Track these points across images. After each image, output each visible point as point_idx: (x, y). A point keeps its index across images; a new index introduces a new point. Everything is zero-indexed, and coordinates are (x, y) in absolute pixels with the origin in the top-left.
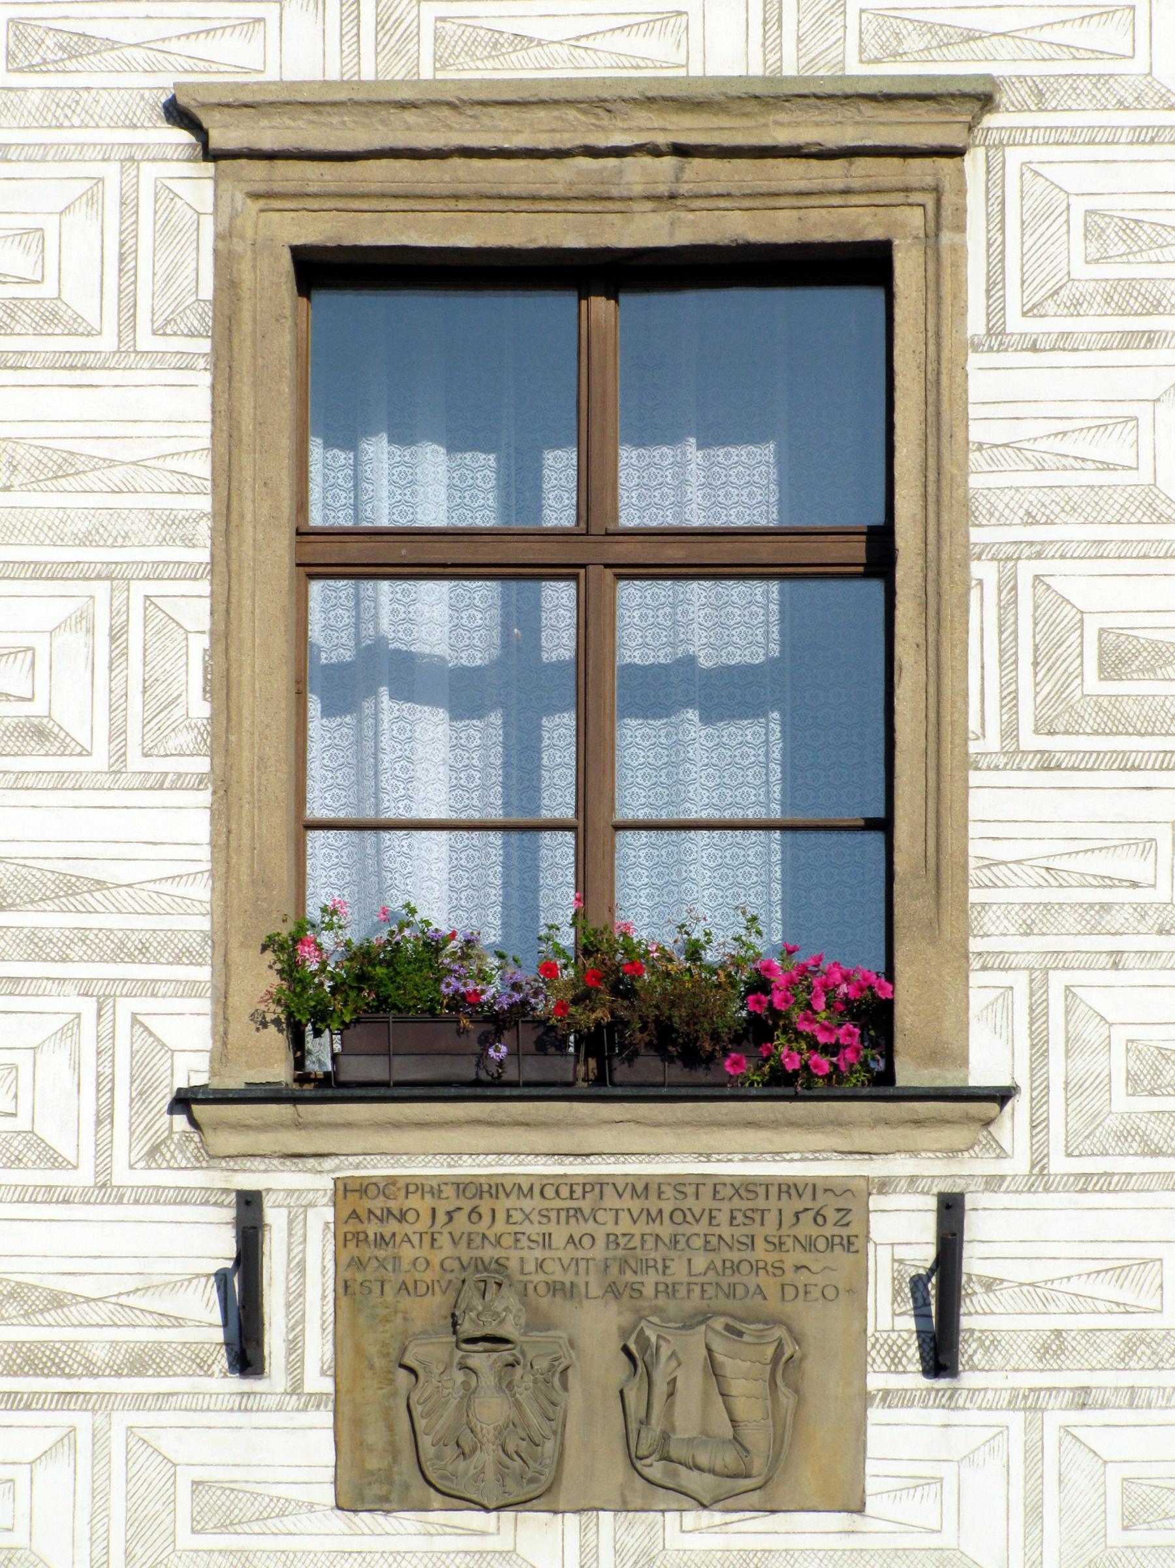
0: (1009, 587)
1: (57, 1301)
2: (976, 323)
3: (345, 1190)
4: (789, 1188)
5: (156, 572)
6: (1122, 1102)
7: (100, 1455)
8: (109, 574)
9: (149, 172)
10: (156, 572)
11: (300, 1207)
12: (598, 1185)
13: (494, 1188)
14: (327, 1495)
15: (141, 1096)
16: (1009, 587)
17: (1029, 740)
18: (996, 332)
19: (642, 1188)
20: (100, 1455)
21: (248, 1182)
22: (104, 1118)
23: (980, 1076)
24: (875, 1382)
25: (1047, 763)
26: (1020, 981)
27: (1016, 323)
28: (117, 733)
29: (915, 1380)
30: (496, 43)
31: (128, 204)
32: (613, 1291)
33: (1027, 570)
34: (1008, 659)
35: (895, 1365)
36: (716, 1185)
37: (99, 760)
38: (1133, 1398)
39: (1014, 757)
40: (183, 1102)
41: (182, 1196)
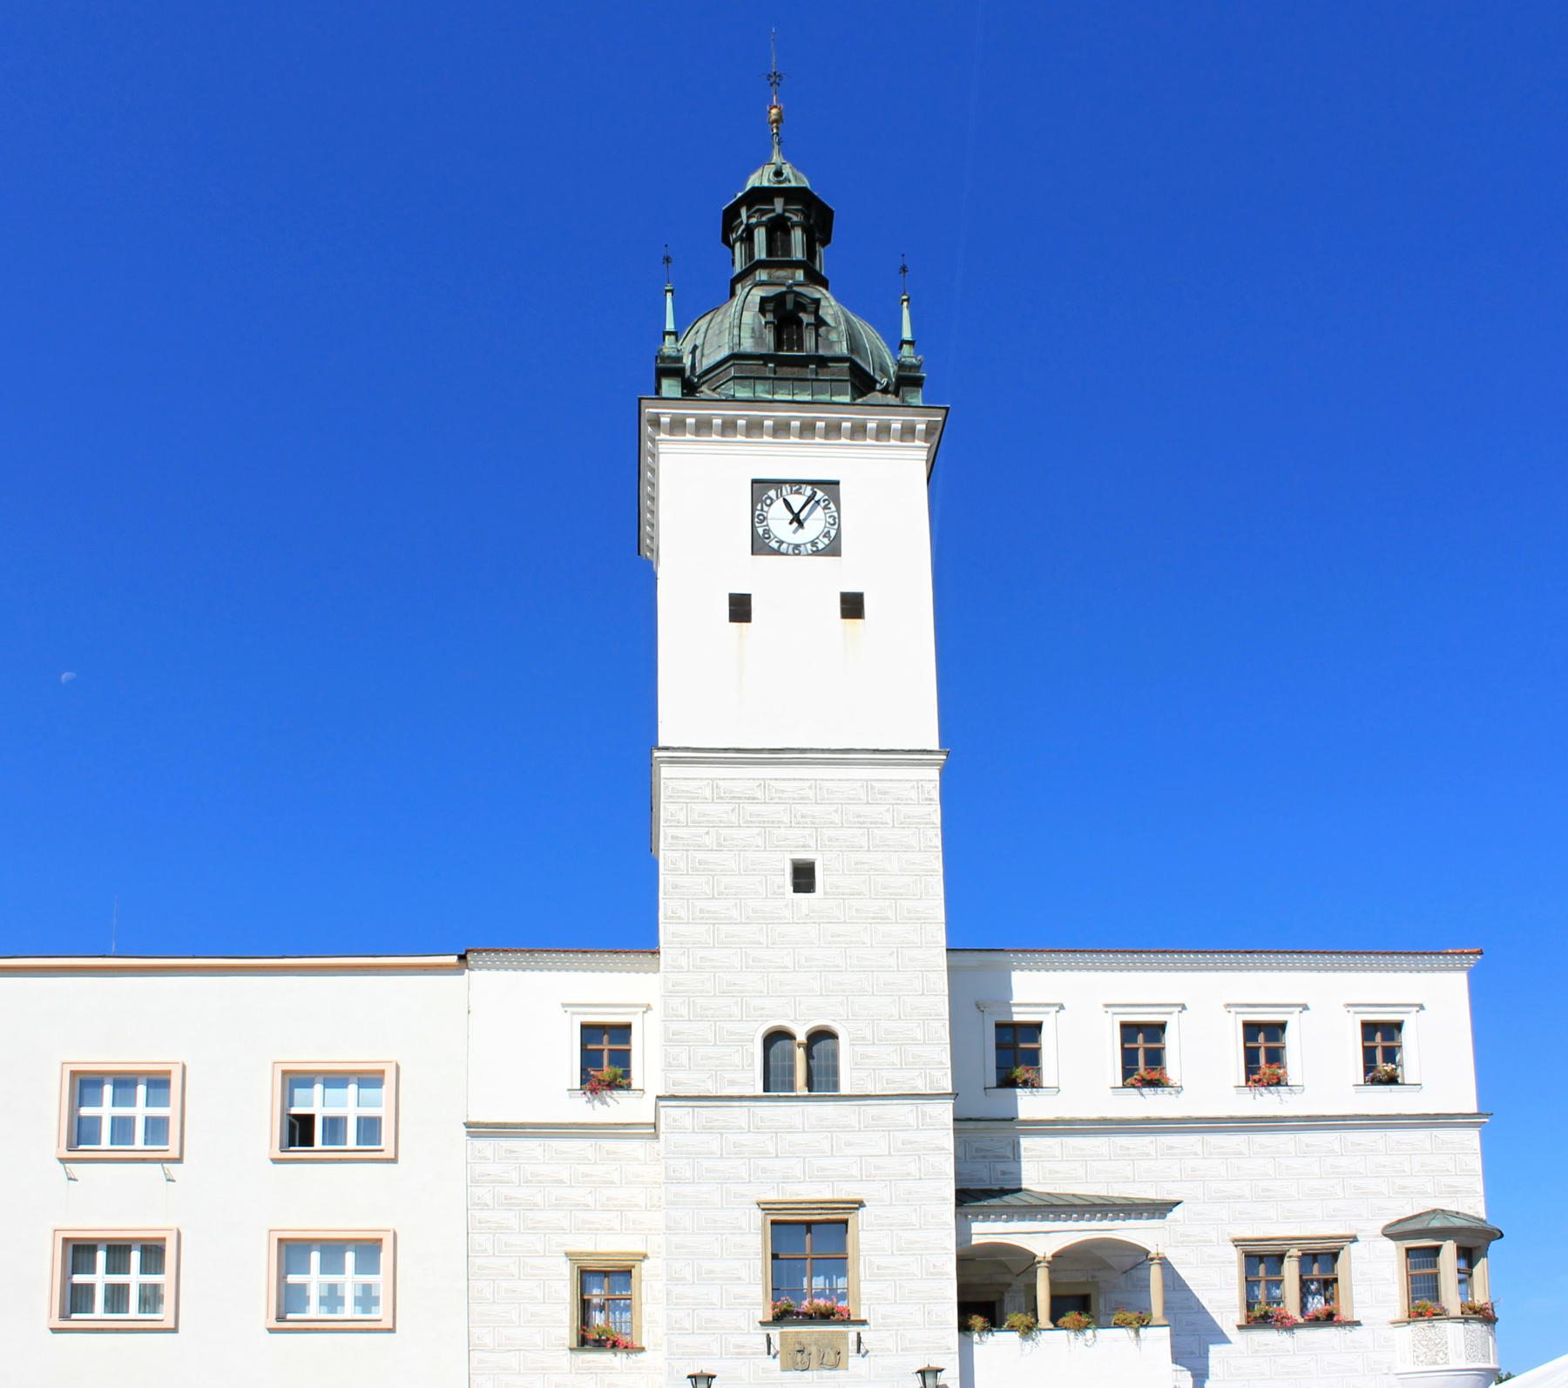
0: (865, 1259)
1: (743, 1346)
2: (860, 1228)
3: (781, 1333)
4: (838, 1332)
5: (754, 1259)
6: (881, 1321)
7: (749, 1365)
8: (748, 1259)
9: (752, 1211)
10: (754, 1259)
11: (774, 1335)
12: (813, 1332)
13: (800, 1332)
14: (779, 1369)
15: (754, 1321)
16: (865, 1259)
17: (868, 1278)
18: (863, 1230)
19: (820, 1332)
20: (749, 1365)
21: (768, 1332)
22: (749, 1325)
23: (863, 1318)
24: (850, 1354)
25: (870, 1280)
26: (867, 1307)
27: (865, 1228)
28: (750, 1278)
29: (855, 1353)
30: (798, 1195)
31: (750, 1214)
32: (815, 1344)
33: (867, 1258)
34: (865, 1268)
35: (852, 1352)
36: (829, 1332)
37: (747, 1281)
38: (882, 1356)
39: (866, 1280)
40: (760, 1322)
41: (759, 1334)
